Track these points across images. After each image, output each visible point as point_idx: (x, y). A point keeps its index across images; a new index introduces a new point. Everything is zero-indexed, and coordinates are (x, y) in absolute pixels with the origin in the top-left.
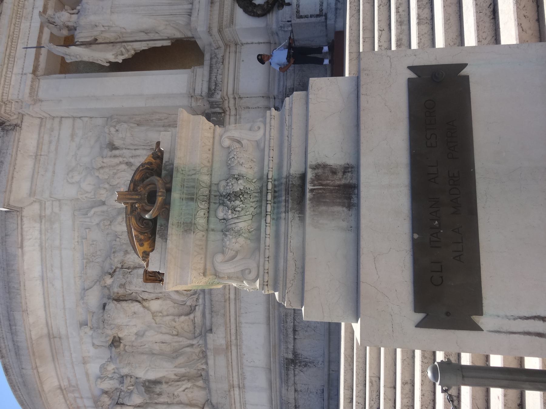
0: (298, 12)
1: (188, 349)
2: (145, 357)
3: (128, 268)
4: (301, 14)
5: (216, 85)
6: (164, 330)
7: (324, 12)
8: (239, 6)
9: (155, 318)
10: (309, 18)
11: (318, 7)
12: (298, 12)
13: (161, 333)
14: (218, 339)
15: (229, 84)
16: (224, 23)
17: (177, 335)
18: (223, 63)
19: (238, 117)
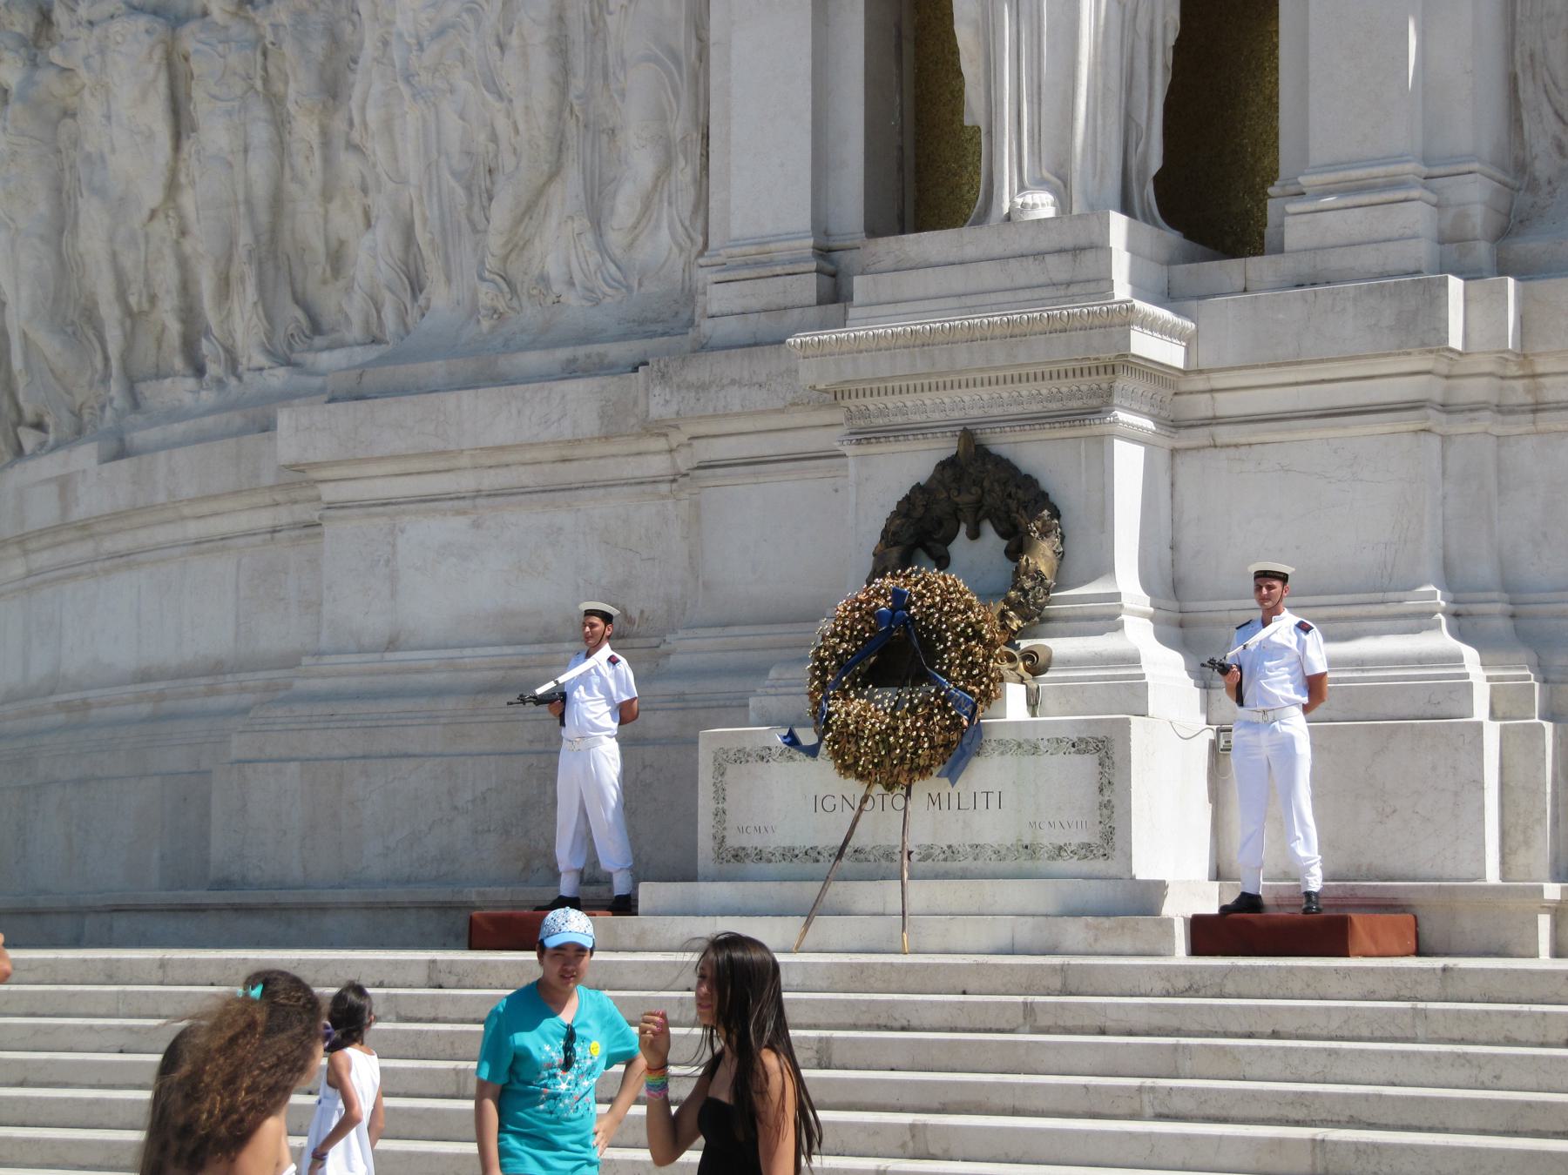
0: (742, 757)
1: (99, 363)
2: (43, 207)
3: (266, 80)
4: (731, 770)
5: (702, 387)
6: (128, 260)
7: (734, 866)
8: (942, 466)
9: (161, 216)
10: (713, 805)
11: (751, 841)
12: (742, 757)
13: (114, 256)
14: (98, 485)
15: (733, 441)
16: (871, 403)
17: (128, 312)
18: (793, 404)
19: (664, 488)
